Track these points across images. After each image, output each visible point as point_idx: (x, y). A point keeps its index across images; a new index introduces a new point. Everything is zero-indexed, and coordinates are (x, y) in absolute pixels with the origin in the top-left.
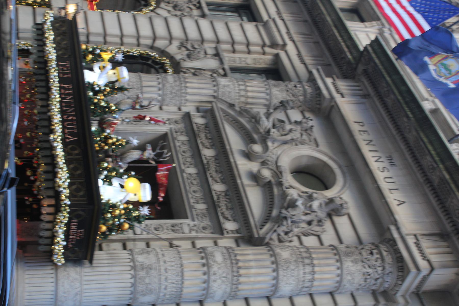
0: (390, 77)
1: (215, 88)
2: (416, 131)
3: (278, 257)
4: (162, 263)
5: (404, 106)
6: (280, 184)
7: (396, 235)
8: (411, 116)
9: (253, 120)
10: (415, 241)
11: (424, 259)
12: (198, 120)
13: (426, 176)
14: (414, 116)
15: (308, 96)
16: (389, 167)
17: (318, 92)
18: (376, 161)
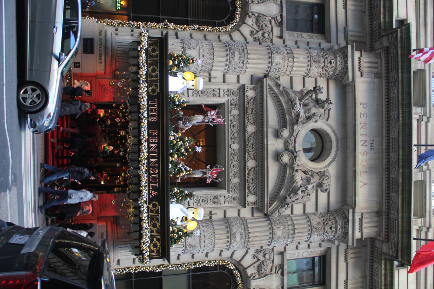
0: (402, 73)
1: (270, 65)
2: (399, 133)
3: (274, 235)
4: (203, 242)
5: (400, 107)
6: (292, 168)
7: (350, 218)
8: (400, 118)
9: (290, 103)
10: (360, 217)
11: (360, 232)
12: (250, 94)
13: (388, 165)
14: (403, 120)
15: (337, 72)
16: (368, 151)
17: (345, 70)
18: (362, 145)
